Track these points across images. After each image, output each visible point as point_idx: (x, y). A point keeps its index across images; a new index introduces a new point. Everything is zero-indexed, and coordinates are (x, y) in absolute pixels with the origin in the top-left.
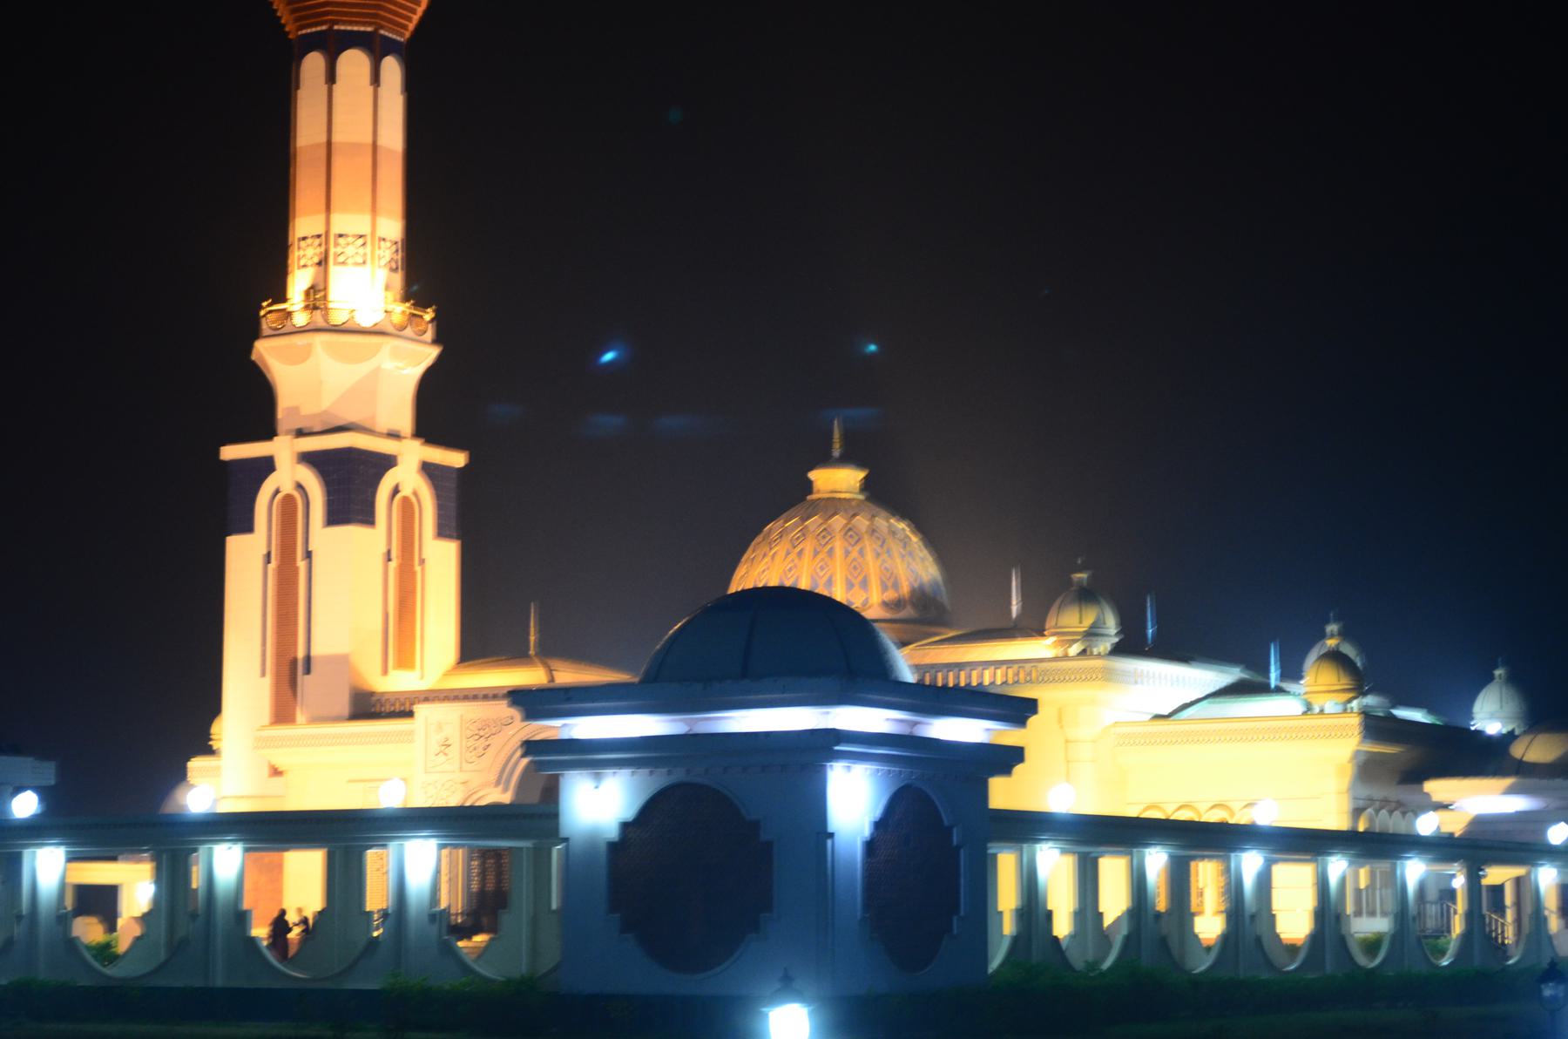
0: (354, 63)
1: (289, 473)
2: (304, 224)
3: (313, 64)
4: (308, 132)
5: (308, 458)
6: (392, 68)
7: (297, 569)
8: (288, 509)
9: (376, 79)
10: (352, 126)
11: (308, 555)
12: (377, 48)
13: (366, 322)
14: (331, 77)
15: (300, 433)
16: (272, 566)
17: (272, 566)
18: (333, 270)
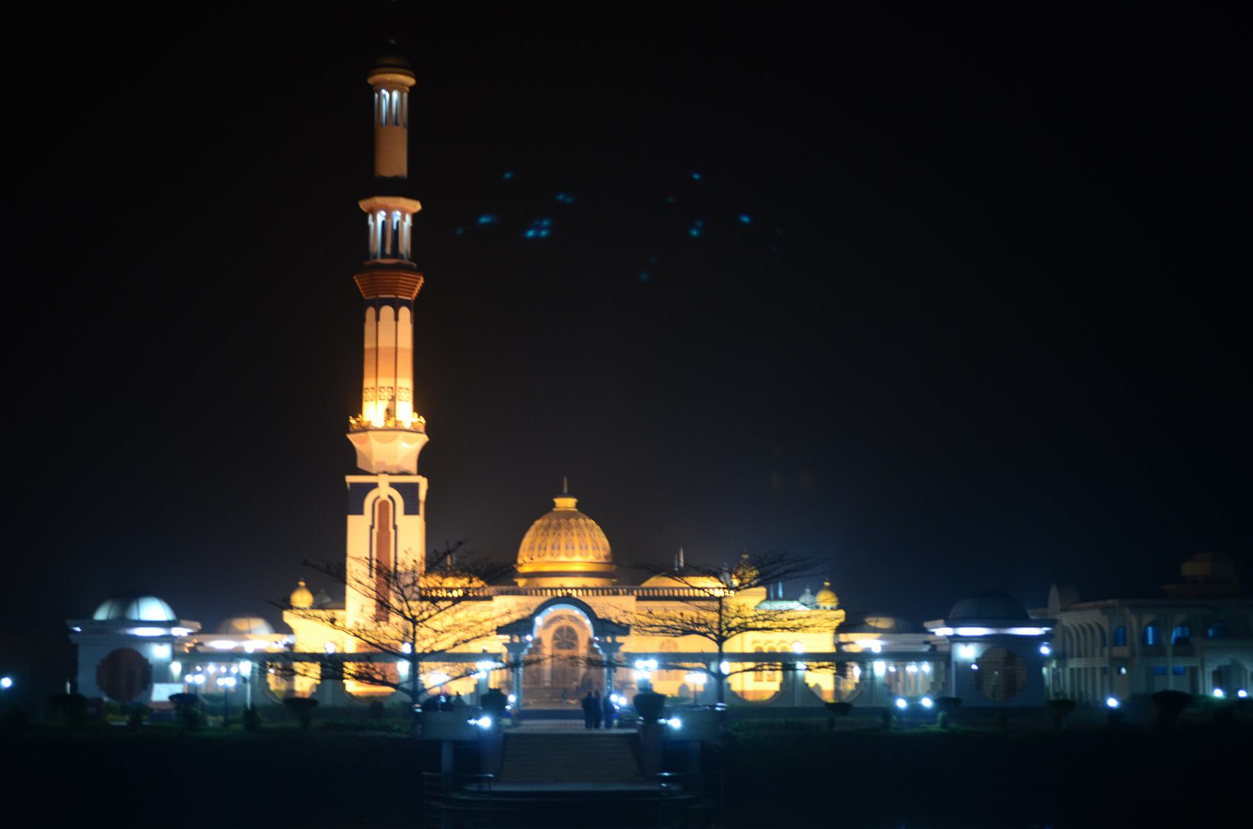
0: (387, 311)
1: (384, 490)
2: (368, 383)
3: (370, 312)
4: (369, 344)
5: (393, 485)
6: (405, 313)
7: (389, 533)
8: (384, 508)
9: (396, 319)
10: (385, 341)
11: (395, 527)
12: (396, 305)
13: (407, 426)
14: (377, 319)
15: (391, 474)
16: (375, 531)
17: (375, 531)
18: (398, 402)
